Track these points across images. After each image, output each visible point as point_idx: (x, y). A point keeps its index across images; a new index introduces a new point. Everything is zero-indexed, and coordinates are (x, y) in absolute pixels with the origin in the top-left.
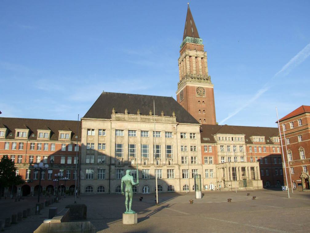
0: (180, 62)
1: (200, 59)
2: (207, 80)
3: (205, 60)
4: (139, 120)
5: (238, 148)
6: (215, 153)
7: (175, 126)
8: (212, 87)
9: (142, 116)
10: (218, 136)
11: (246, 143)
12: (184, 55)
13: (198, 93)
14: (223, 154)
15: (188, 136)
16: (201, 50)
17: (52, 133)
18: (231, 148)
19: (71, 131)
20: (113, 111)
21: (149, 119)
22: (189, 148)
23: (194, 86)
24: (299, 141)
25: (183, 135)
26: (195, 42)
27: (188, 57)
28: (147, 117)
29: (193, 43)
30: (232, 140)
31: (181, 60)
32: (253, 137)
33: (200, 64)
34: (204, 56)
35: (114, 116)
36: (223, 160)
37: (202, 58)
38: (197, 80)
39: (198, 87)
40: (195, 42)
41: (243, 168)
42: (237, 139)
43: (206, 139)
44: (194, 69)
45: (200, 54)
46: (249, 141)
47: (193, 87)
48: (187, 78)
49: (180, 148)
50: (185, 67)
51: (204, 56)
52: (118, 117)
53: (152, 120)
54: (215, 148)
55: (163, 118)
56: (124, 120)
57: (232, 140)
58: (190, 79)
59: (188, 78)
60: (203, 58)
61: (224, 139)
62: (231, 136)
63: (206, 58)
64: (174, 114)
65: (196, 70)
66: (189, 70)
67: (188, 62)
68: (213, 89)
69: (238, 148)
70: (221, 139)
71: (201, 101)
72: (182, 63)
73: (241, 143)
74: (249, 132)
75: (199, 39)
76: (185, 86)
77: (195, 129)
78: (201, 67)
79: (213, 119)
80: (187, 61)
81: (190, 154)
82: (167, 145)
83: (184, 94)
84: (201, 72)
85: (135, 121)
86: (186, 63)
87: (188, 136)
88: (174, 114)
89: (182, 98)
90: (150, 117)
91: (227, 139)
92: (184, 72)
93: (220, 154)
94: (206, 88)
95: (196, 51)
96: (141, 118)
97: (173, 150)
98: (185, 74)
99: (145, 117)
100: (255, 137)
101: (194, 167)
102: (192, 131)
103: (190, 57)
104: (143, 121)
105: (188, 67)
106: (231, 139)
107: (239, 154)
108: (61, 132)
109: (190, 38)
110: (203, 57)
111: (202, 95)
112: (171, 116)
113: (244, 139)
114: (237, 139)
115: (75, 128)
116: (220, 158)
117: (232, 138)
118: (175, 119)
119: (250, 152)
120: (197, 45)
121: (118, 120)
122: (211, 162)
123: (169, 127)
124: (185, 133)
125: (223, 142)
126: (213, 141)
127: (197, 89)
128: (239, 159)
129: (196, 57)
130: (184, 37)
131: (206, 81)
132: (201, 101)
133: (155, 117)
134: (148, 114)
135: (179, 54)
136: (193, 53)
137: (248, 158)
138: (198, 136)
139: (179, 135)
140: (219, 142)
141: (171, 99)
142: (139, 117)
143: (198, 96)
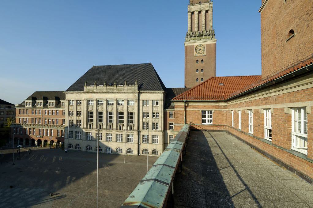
1: (203, 13)
4: (105, 90)
21: (113, 89)
23: (192, 45)
28: (112, 87)
34: (210, 7)
35: (85, 88)
37: (207, 11)
51: (210, 7)
52: (89, 90)
53: (115, 90)
56: (92, 92)
60: (208, 10)
63: (211, 9)
78: (204, 22)
94: (206, 45)
110: (207, 9)
111: (201, 53)
112: (135, 84)
121: (88, 92)
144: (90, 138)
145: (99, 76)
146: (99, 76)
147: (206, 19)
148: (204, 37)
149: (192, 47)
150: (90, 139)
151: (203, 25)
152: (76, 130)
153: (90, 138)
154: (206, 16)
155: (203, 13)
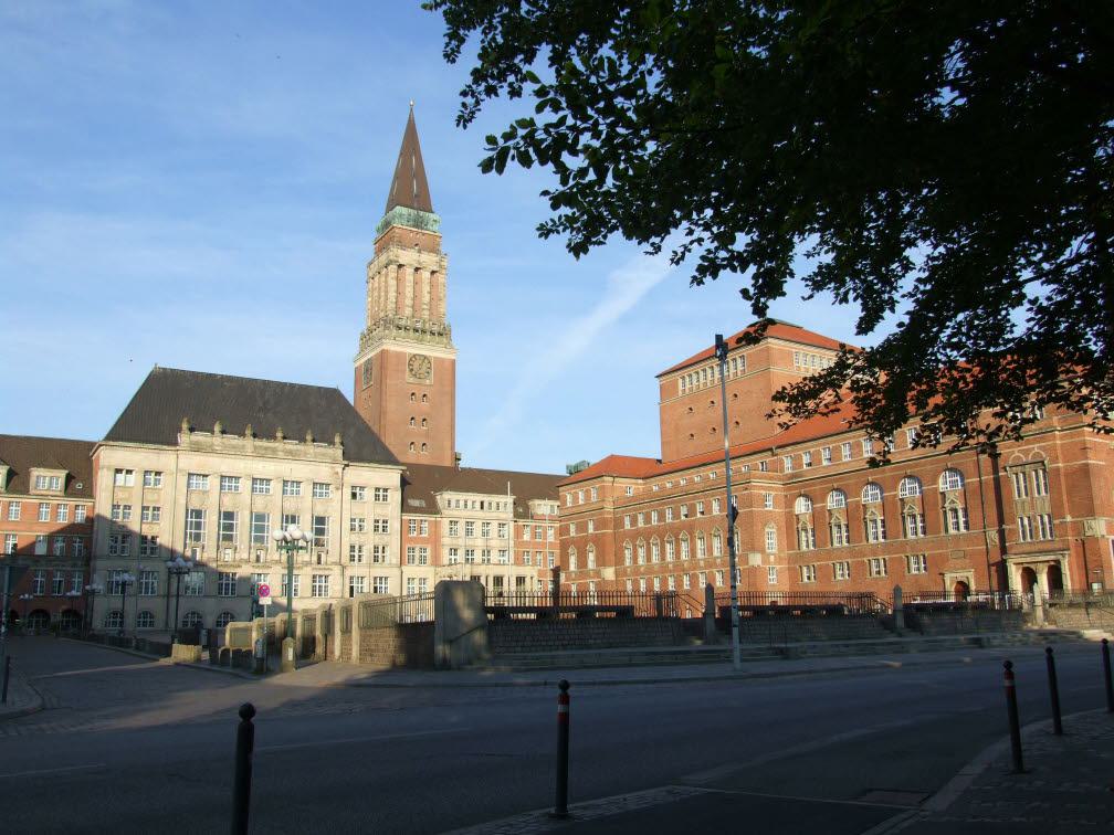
0: (371, 275)
1: (426, 275)
2: (440, 334)
3: (441, 278)
4: (249, 449)
5: (494, 527)
6: (435, 540)
7: (340, 470)
9: (258, 443)
10: (444, 498)
11: (517, 515)
12: (383, 258)
13: (412, 370)
14: (454, 542)
15: (369, 494)
16: (434, 250)
17: (11, 475)
18: (478, 528)
19: (65, 468)
20: (185, 426)
21: (274, 450)
22: (369, 526)
24: (714, 513)
25: (358, 491)
26: (419, 223)
27: (393, 267)
29: (413, 226)
30: (482, 508)
31: (374, 268)
32: (537, 502)
33: (426, 288)
34: (441, 266)
35: (185, 438)
36: (453, 557)
37: (433, 272)
38: (411, 332)
39: (414, 356)
40: (419, 223)
41: (498, 578)
42: (494, 505)
43: (415, 503)
44: (409, 302)
45: (429, 260)
46: (522, 512)
47: (399, 355)
48: (386, 328)
49: (347, 525)
50: (383, 294)
51: (441, 266)
52: (197, 443)
54: (436, 525)
55: (311, 449)
56: (210, 450)
57: (482, 508)
58: (395, 332)
59: (388, 328)
61: (462, 503)
62: (478, 498)
63: (444, 271)
64: (337, 440)
65: (413, 307)
66: (394, 306)
67: (392, 282)
68: (453, 362)
69: (494, 527)
70: (453, 504)
71: (419, 395)
72: (376, 279)
73: (503, 516)
74: (527, 488)
76: (379, 350)
77: (390, 477)
78: (426, 298)
79: (447, 444)
80: (389, 279)
81: (369, 540)
82: (316, 514)
83: (372, 373)
84: (427, 313)
85: (239, 452)
86: (386, 282)
87: (369, 494)
88: (337, 440)
89: (368, 380)
90: (278, 445)
91: (470, 504)
92: (379, 307)
93: (447, 541)
95: (419, 251)
96: (255, 447)
97: (332, 527)
98: (382, 314)
99: (264, 443)
100: (542, 502)
101: (378, 571)
102: (381, 484)
103: (400, 266)
104: (260, 454)
105: (392, 295)
106: (478, 505)
107: (495, 543)
108: (36, 472)
109: (404, 210)
110: (435, 269)
112: (331, 443)
113: (510, 507)
114: (494, 505)
115: (76, 462)
116: (445, 552)
117: (482, 503)
118: (340, 452)
119: (527, 537)
120: (424, 234)
121: (197, 448)
122: (423, 560)
123: (324, 472)
124: (362, 488)
125: (456, 513)
126: (432, 508)
127: (411, 360)
128: (495, 556)
129: (417, 269)
130: (390, 208)
131: (437, 338)
132: (419, 395)
133: (291, 445)
135: (372, 248)
136: (408, 257)
137: (516, 553)
138: (395, 497)
139: (347, 492)
140: (446, 512)
141: (333, 395)
142: (249, 443)
143: (411, 380)
144: (147, 588)
145: (169, 407)
146: (169, 407)
150: (147, 592)
151: (425, 307)
152: (141, 567)
153: (147, 588)
155: (426, 275)
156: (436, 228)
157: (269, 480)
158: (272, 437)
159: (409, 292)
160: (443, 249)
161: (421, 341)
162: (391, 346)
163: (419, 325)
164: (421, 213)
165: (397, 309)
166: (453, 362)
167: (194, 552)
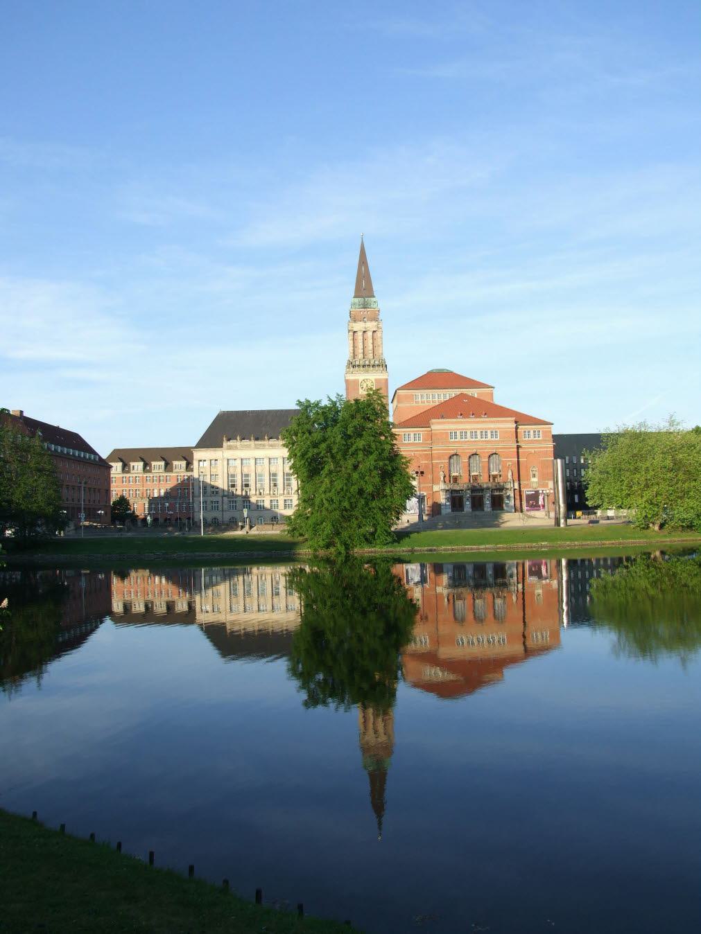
1: (370, 334)
3: (378, 334)
8: (385, 377)
9: (257, 442)
20: (225, 439)
21: (264, 445)
26: (365, 306)
28: (262, 442)
29: (365, 308)
34: (378, 328)
35: (225, 444)
37: (374, 332)
38: (361, 368)
40: (365, 306)
45: (371, 325)
51: (378, 328)
52: (230, 446)
56: (236, 448)
68: (387, 380)
75: (373, 299)
78: (371, 347)
84: (372, 355)
85: (248, 447)
90: (266, 442)
94: (376, 380)
104: (257, 447)
121: (230, 448)
129: (364, 332)
134: (263, 439)
142: (253, 443)
147: (373, 344)
148: (371, 368)
149: (356, 382)
154: (373, 338)
156: (375, 306)
157: (277, 458)
158: (264, 439)
159: (360, 346)
160: (380, 317)
161: (367, 372)
162: (351, 377)
163: (367, 363)
164: (366, 299)
165: (354, 356)
166: (387, 380)
167: (247, 492)
